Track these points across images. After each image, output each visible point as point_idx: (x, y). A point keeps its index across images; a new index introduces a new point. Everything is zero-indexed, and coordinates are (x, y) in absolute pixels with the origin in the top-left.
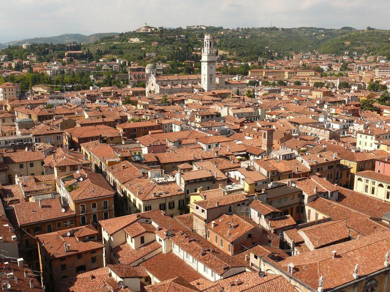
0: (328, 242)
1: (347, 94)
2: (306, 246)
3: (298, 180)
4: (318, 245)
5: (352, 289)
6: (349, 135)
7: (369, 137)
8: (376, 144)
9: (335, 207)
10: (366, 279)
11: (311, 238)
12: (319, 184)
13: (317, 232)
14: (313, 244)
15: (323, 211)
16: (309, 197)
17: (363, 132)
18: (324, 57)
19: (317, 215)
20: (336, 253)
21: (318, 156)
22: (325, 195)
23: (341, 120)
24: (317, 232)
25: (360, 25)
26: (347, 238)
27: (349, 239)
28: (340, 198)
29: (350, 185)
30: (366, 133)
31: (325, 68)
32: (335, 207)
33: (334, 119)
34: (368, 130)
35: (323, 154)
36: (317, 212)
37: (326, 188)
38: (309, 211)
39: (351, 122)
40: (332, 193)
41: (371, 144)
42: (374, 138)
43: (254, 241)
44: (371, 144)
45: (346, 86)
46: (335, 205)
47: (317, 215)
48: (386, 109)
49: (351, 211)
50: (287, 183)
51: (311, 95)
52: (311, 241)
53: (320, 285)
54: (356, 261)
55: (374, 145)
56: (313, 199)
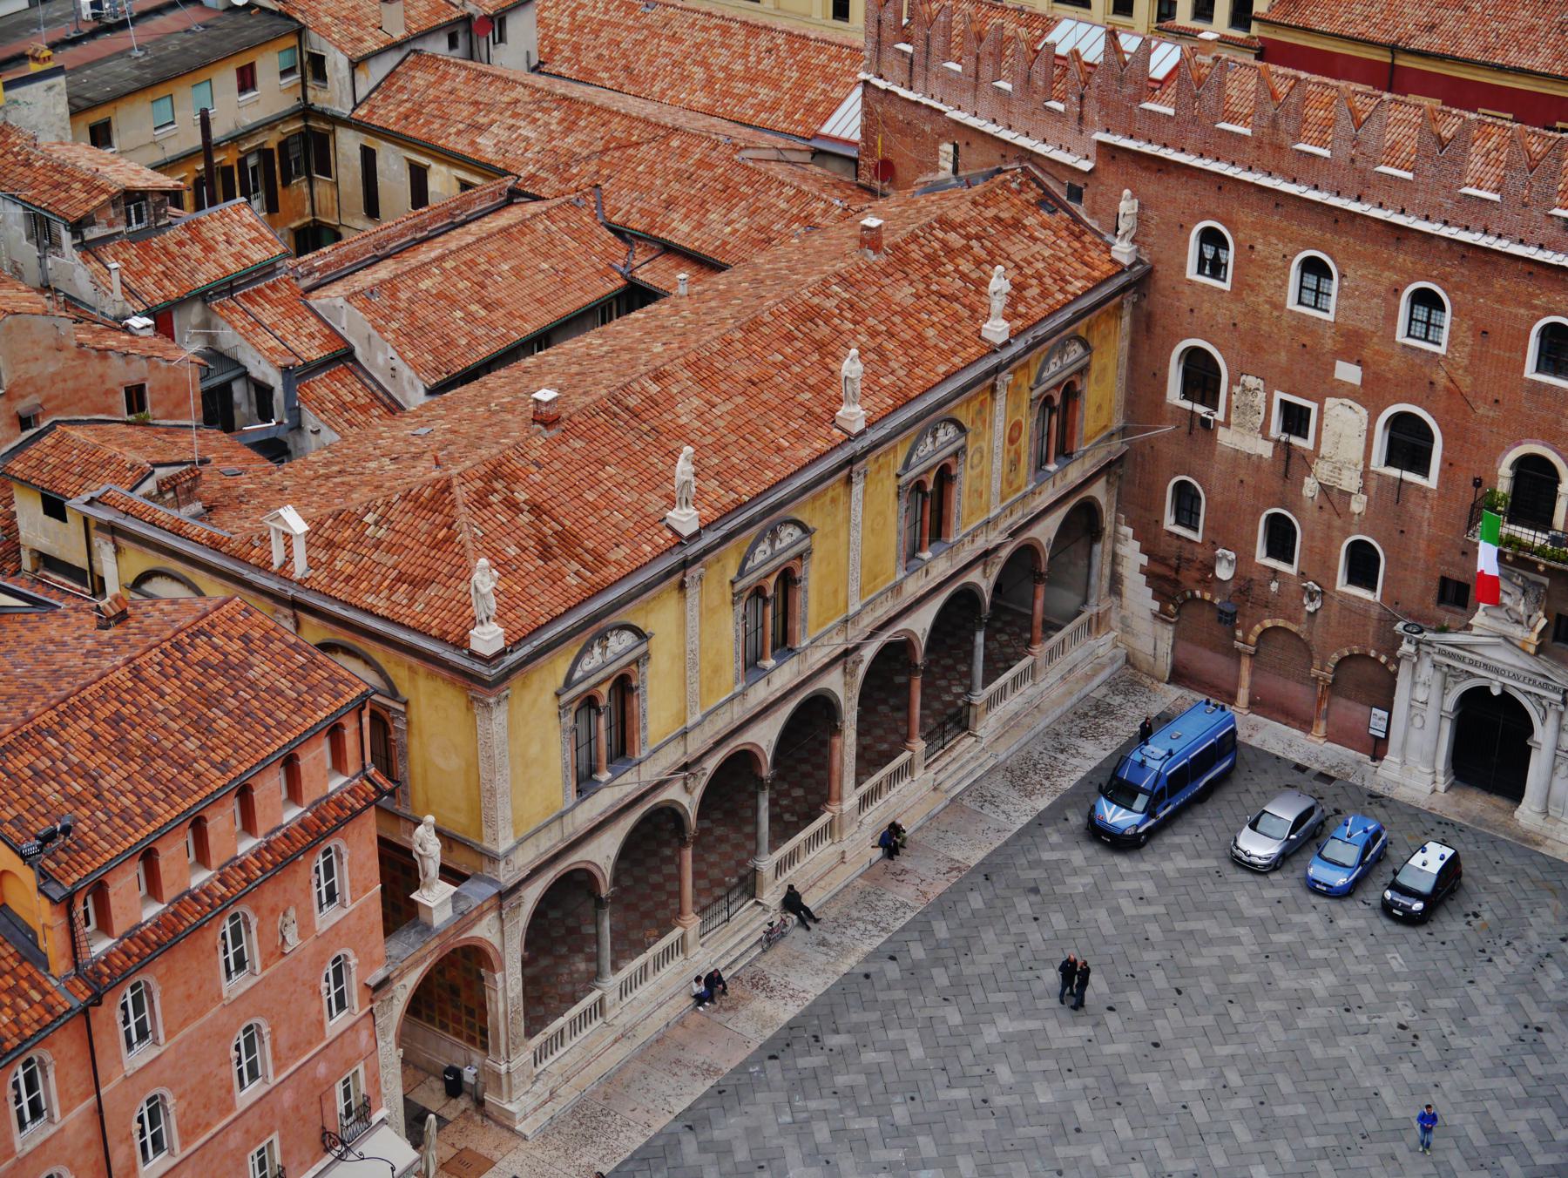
16: (355, 65)
19: (419, 176)
38: (368, 156)
43: (22, 406)
47: (419, 176)
54: (682, 434)
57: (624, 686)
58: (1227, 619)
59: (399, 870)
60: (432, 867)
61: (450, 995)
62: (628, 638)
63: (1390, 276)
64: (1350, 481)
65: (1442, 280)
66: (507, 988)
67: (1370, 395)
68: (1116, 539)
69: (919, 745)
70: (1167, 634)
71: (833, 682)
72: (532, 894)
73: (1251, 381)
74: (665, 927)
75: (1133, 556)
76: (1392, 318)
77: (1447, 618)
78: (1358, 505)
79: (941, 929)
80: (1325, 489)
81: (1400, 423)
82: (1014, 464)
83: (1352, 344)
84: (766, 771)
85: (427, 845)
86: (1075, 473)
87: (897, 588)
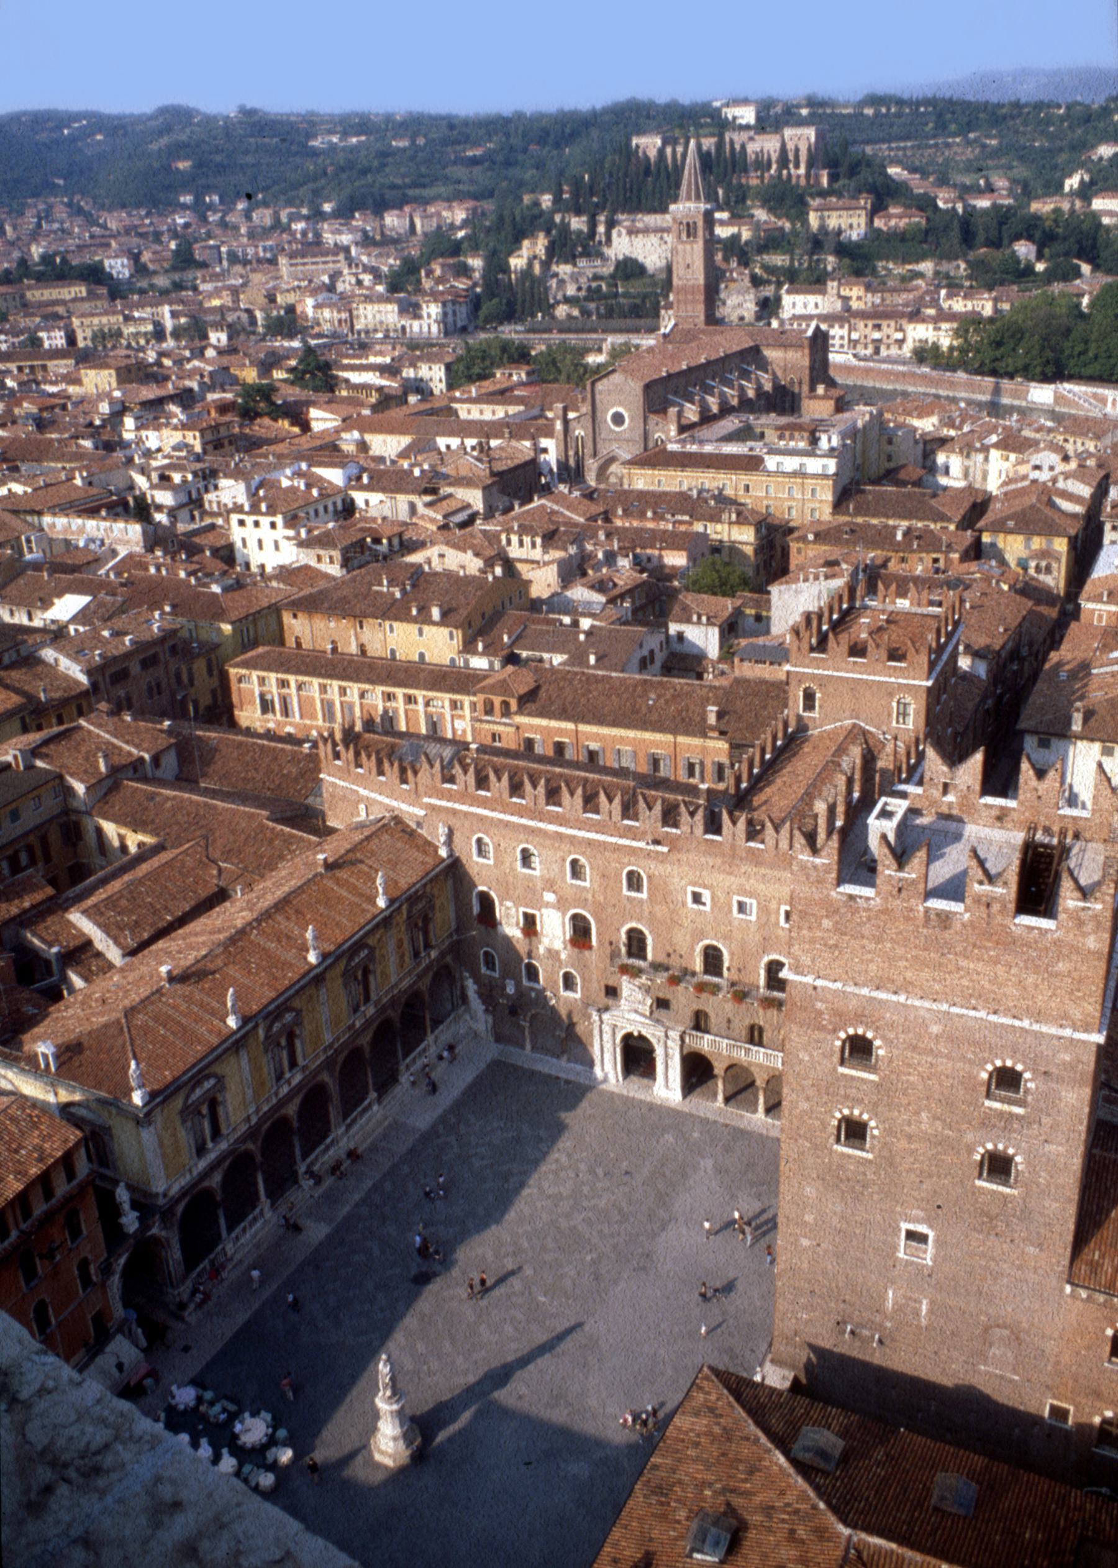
0: (161, 924)
1: (196, 363)
2: (99, 955)
3: (46, 742)
4: (132, 943)
5: (233, 1060)
6: (208, 521)
7: (265, 521)
8: (288, 538)
9: (169, 804)
10: (265, 1018)
11: (105, 928)
12: (109, 738)
13: (124, 903)
14: (117, 943)
15: (137, 825)
17: (247, 508)
18: (114, 221)
20: (169, 972)
21: (106, 633)
22: (135, 770)
23: (177, 478)
24: (124, 903)
25: (218, 98)
26: (215, 895)
27: (221, 896)
28: (188, 765)
29: (220, 710)
30: (255, 510)
31: (118, 266)
32: (169, 804)
33: (155, 476)
34: (260, 500)
35: (119, 623)
36: (123, 831)
37: (137, 746)
39: (209, 477)
40: (156, 760)
41: (276, 543)
42: (279, 519)
44: (276, 543)
45: (195, 331)
46: (167, 799)
48: (314, 404)
49: (215, 807)
50: (9, 758)
51: (78, 382)
52: (108, 934)
53: (133, 1084)
55: (283, 544)
56: (107, 789)
57: (213, 1104)
58: (514, 1011)
59: (110, 1211)
60: (126, 1206)
61: (145, 1259)
62: (212, 1081)
63: (559, 854)
64: (558, 945)
65: (583, 854)
66: (175, 1254)
67: (561, 905)
68: (462, 979)
69: (373, 1095)
70: (490, 1019)
71: (325, 1077)
72: (180, 1208)
73: (509, 904)
74: (254, 1207)
75: (471, 987)
76: (563, 871)
77: (610, 1002)
78: (563, 956)
79: (388, 1186)
80: (549, 951)
81: (575, 917)
82: (402, 956)
83: (550, 885)
84: (295, 1124)
85: (123, 1195)
86: (434, 954)
87: (350, 1028)
